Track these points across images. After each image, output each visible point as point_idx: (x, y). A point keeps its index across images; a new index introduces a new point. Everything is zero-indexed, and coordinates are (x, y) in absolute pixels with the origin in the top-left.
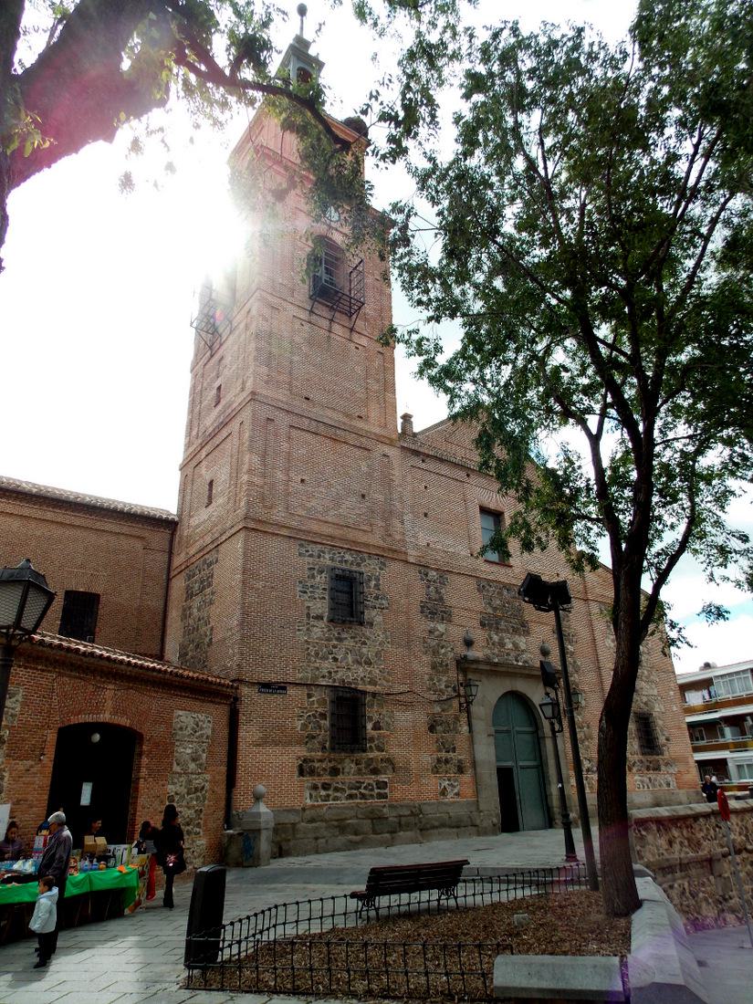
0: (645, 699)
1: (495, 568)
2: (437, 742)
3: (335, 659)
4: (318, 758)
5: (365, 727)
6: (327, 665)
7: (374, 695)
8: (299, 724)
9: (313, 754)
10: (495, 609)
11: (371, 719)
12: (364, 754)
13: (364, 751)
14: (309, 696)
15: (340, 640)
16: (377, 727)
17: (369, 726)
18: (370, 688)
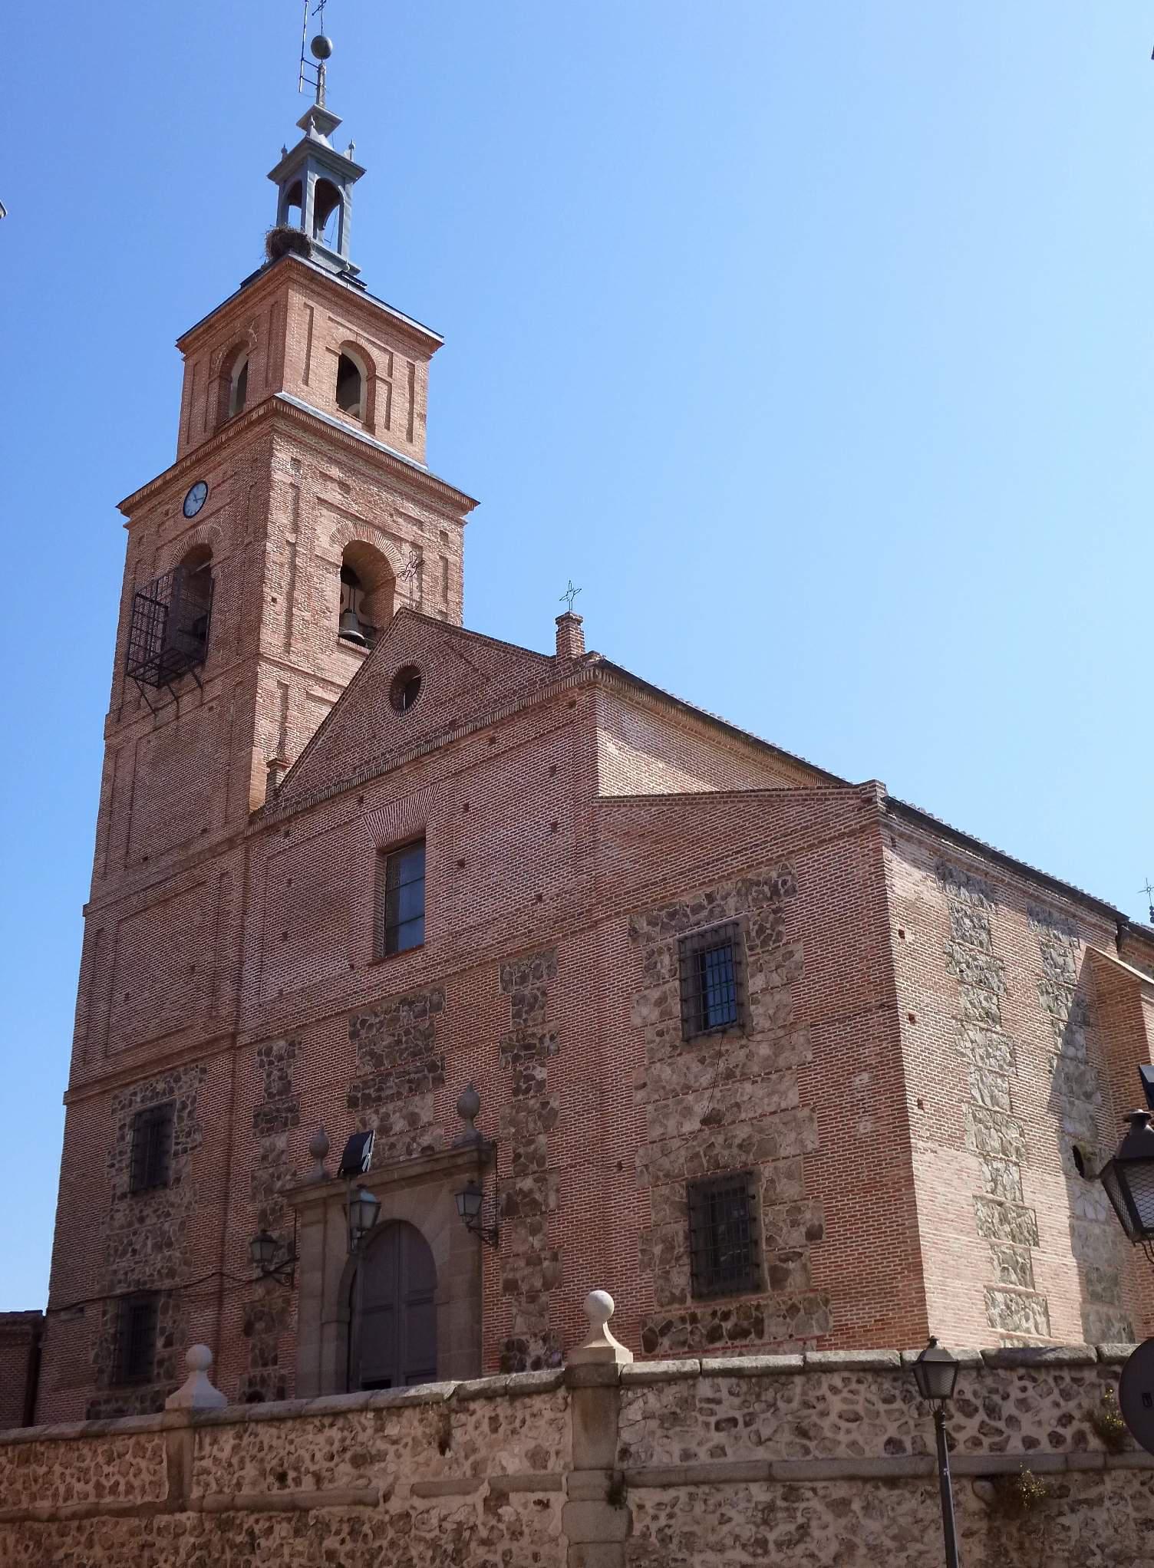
0: (742, 1133)
1: (392, 968)
2: (253, 1349)
3: (134, 1251)
4: (104, 1397)
5: (153, 1345)
6: (124, 1263)
7: (170, 1293)
8: (92, 1355)
9: (100, 1393)
10: (377, 1060)
11: (163, 1329)
12: (149, 1386)
13: (149, 1381)
14: (104, 1313)
15: (142, 1220)
16: (169, 1343)
17: (160, 1343)
18: (167, 1284)
